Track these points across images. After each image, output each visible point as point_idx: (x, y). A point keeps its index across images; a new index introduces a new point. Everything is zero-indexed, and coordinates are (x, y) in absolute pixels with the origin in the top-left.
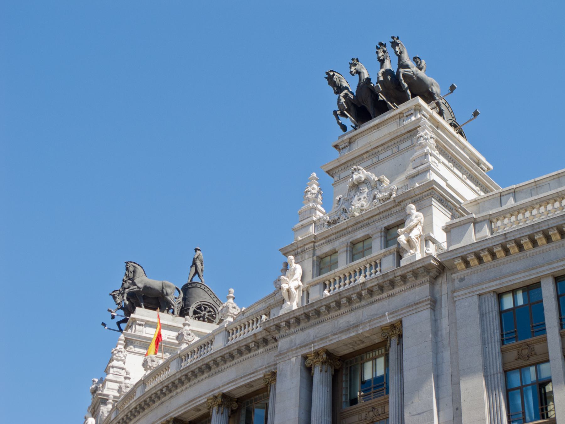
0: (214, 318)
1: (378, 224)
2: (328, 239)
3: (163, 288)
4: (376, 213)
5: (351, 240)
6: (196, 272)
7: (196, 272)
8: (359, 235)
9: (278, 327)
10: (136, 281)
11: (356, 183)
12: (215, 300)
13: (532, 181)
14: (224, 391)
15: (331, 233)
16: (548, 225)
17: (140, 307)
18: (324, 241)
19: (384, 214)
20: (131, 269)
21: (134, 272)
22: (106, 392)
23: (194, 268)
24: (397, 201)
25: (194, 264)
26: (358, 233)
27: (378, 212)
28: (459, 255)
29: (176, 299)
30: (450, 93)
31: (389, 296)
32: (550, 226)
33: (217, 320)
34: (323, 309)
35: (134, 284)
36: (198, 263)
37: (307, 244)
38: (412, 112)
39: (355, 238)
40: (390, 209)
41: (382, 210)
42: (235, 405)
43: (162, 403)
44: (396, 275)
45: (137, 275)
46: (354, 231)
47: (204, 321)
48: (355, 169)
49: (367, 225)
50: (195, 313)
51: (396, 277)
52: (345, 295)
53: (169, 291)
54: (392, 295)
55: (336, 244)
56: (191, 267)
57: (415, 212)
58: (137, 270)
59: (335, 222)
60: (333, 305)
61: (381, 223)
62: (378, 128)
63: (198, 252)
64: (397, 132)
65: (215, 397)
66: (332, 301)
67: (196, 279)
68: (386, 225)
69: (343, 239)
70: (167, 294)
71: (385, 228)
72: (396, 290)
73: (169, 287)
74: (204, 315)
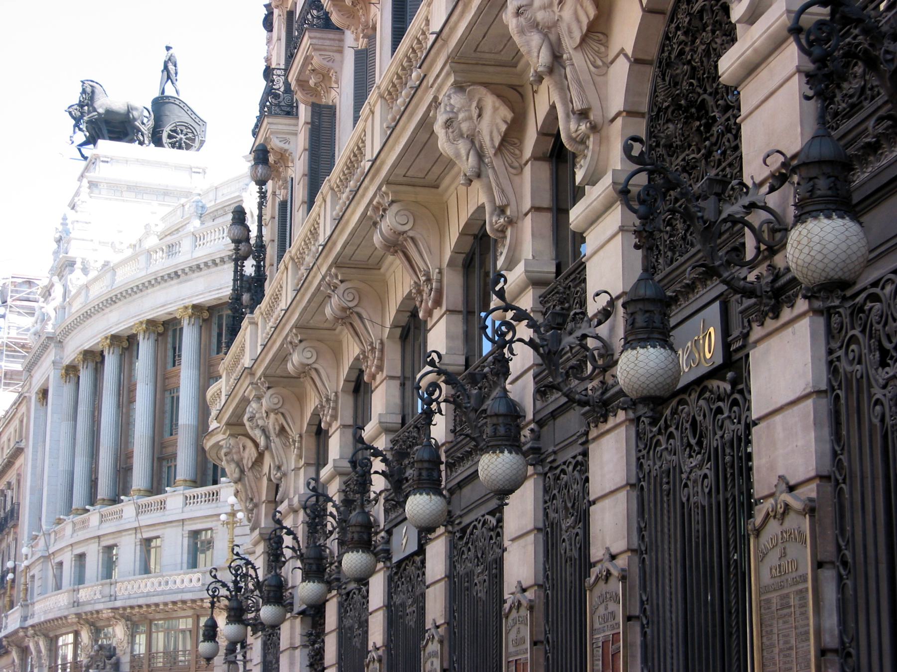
0: (193, 140)
3: (129, 112)
6: (169, 78)
7: (169, 78)
10: (97, 104)
12: (193, 116)
14: (195, 302)
17: (104, 138)
20: (89, 90)
21: (93, 92)
22: (71, 254)
23: (166, 73)
25: (166, 67)
29: (146, 124)
33: (197, 144)
35: (95, 110)
36: (171, 67)
42: (206, 315)
43: (134, 300)
45: (96, 97)
47: (180, 147)
50: (170, 137)
53: (136, 114)
56: (163, 71)
58: (96, 91)
63: (171, 51)
65: (186, 308)
67: (170, 91)
70: (135, 119)
73: (136, 109)
74: (181, 139)
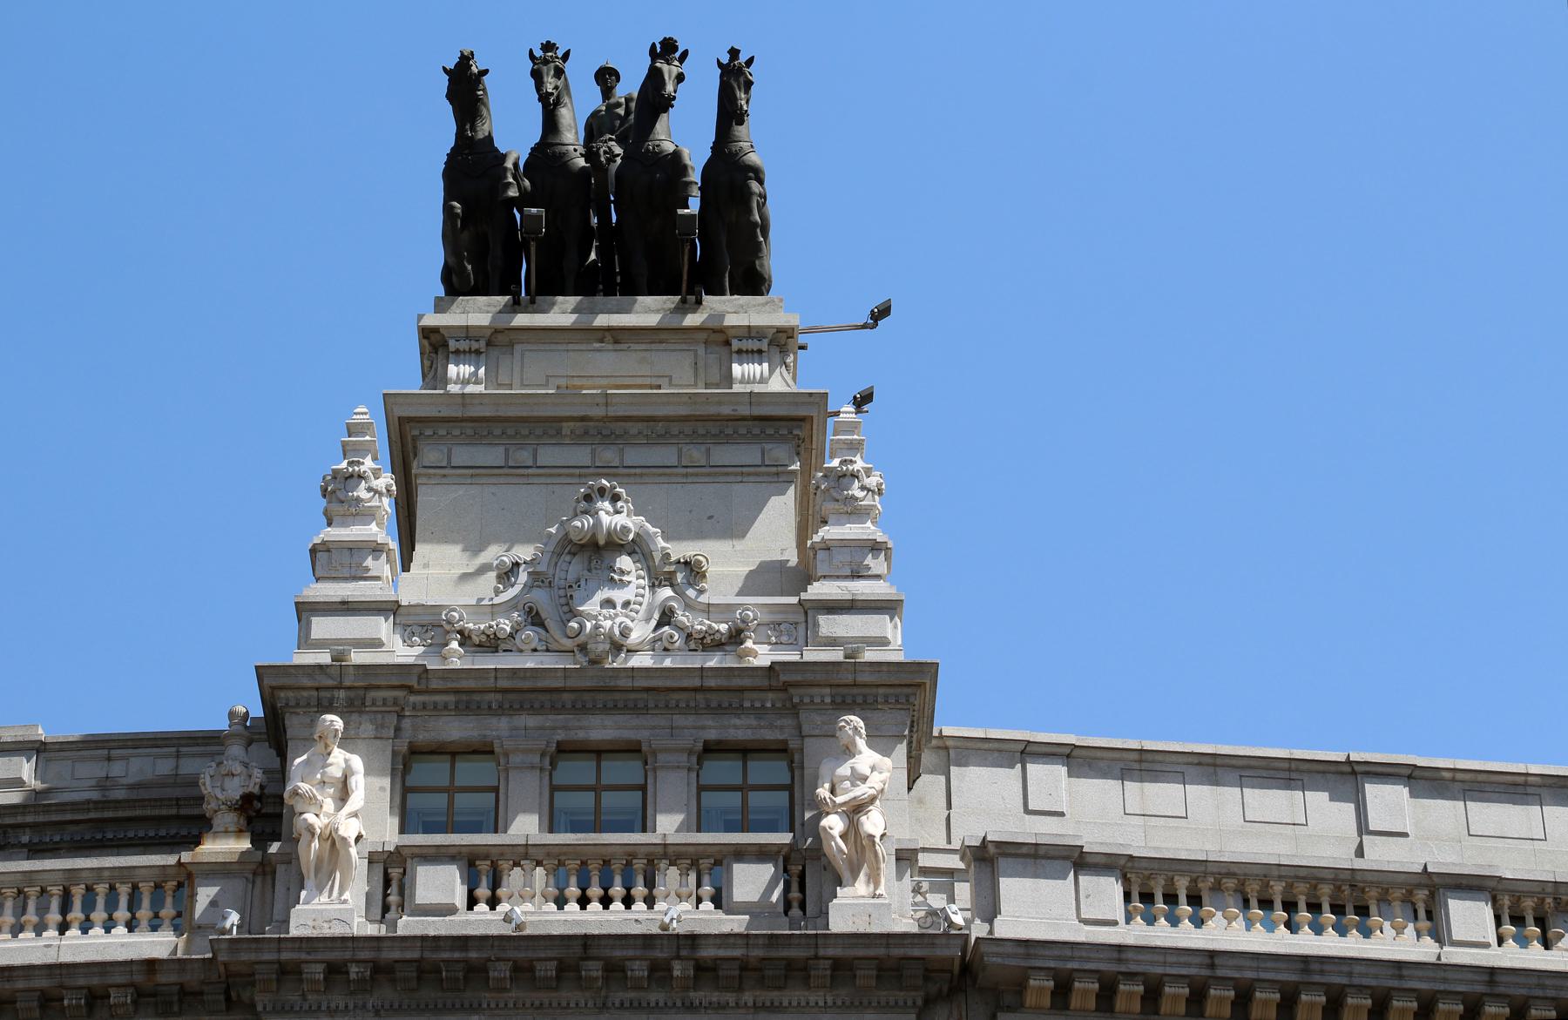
1: (679, 720)
2: (467, 694)
4: (686, 683)
5: (560, 736)
8: (601, 729)
9: (288, 972)
11: (602, 542)
13: (1136, 746)
15: (491, 683)
16: (1350, 974)
18: (451, 698)
19: (714, 699)
24: (783, 678)
26: (595, 720)
27: (697, 683)
28: (1052, 964)
30: (864, 326)
31: (757, 1008)
32: (1356, 981)
34: (501, 971)
37: (378, 687)
38: (764, 345)
39: (581, 735)
40: (742, 690)
41: (712, 683)
44: (821, 952)
46: (581, 709)
48: (602, 492)
49: (635, 709)
51: (816, 957)
52: (608, 953)
54: (773, 1008)
55: (498, 728)
57: (861, 743)
59: (492, 643)
60: (547, 969)
61: (690, 720)
62: (616, 342)
64: (720, 403)
66: (550, 954)
68: (712, 735)
69: (532, 721)
71: (706, 743)
72: (794, 995)
